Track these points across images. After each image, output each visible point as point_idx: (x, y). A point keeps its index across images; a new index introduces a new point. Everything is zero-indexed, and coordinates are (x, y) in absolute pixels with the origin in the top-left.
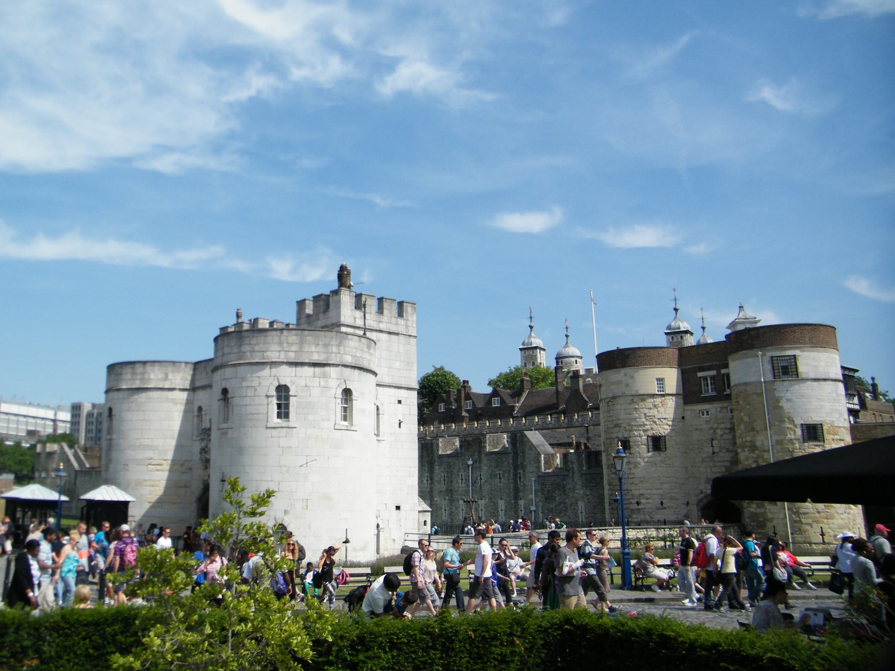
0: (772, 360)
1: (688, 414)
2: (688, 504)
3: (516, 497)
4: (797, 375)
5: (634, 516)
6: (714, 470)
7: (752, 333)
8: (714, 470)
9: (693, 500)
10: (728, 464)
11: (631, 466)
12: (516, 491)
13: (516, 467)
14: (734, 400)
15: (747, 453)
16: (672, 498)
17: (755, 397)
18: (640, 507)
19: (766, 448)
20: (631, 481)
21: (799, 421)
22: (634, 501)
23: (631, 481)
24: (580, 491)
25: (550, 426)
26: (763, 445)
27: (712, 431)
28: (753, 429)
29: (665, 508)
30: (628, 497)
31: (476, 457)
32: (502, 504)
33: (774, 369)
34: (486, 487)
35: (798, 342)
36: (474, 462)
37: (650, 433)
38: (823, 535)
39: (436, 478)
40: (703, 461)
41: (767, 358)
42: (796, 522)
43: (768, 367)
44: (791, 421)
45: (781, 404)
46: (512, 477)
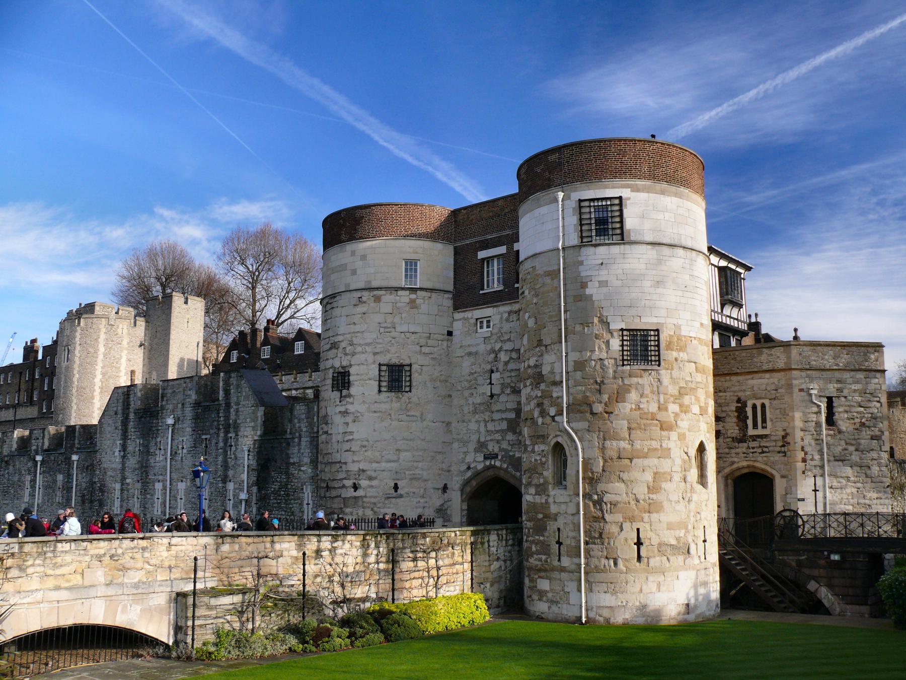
0: (580, 207)
1: (457, 328)
2: (445, 488)
3: (225, 479)
4: (622, 234)
5: (348, 510)
6: (490, 426)
7: (553, 158)
8: (490, 426)
9: (455, 484)
10: (512, 415)
11: (349, 419)
12: (226, 466)
14: (520, 292)
15: (529, 389)
16: (413, 479)
17: (548, 280)
18: (360, 493)
19: (558, 379)
20: (346, 446)
21: (617, 325)
22: (349, 483)
23: (346, 446)
26: (552, 372)
27: (493, 356)
28: (540, 343)
29: (401, 496)
30: (341, 476)
31: (179, 413)
33: (581, 225)
35: (623, 172)
36: (177, 420)
37: (384, 359)
38: (639, 543)
39: (130, 449)
40: (475, 412)
41: (572, 204)
42: (596, 519)
43: (573, 220)
44: (605, 323)
45: (588, 291)
46: (221, 444)
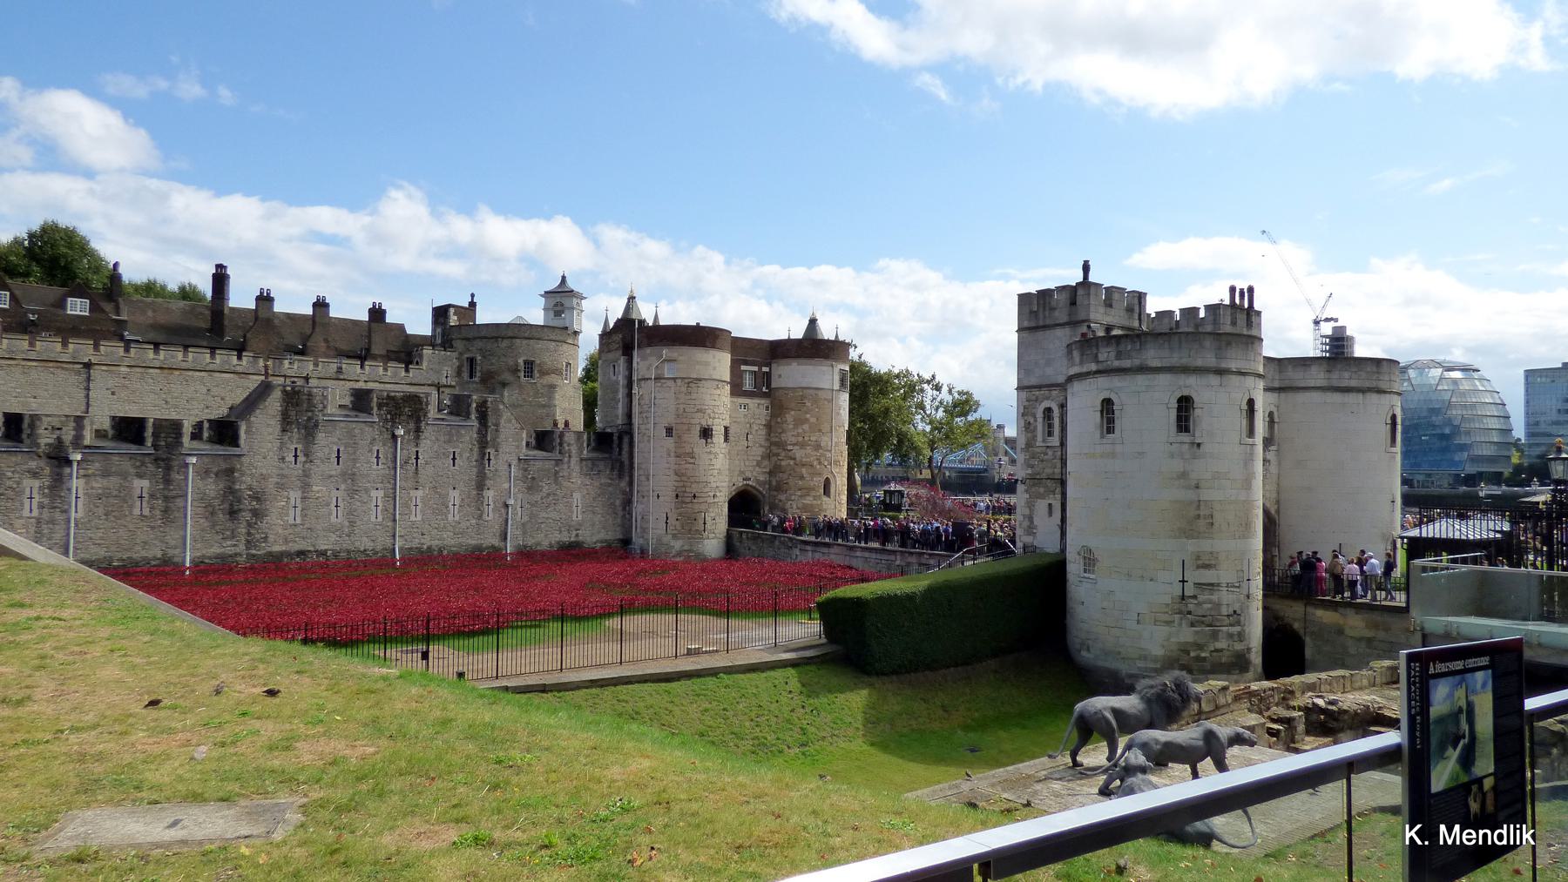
13: (483, 444)
24: (577, 479)
25: (239, 369)
32: (455, 496)
34: (426, 472)
41: (836, 370)
43: (837, 378)
